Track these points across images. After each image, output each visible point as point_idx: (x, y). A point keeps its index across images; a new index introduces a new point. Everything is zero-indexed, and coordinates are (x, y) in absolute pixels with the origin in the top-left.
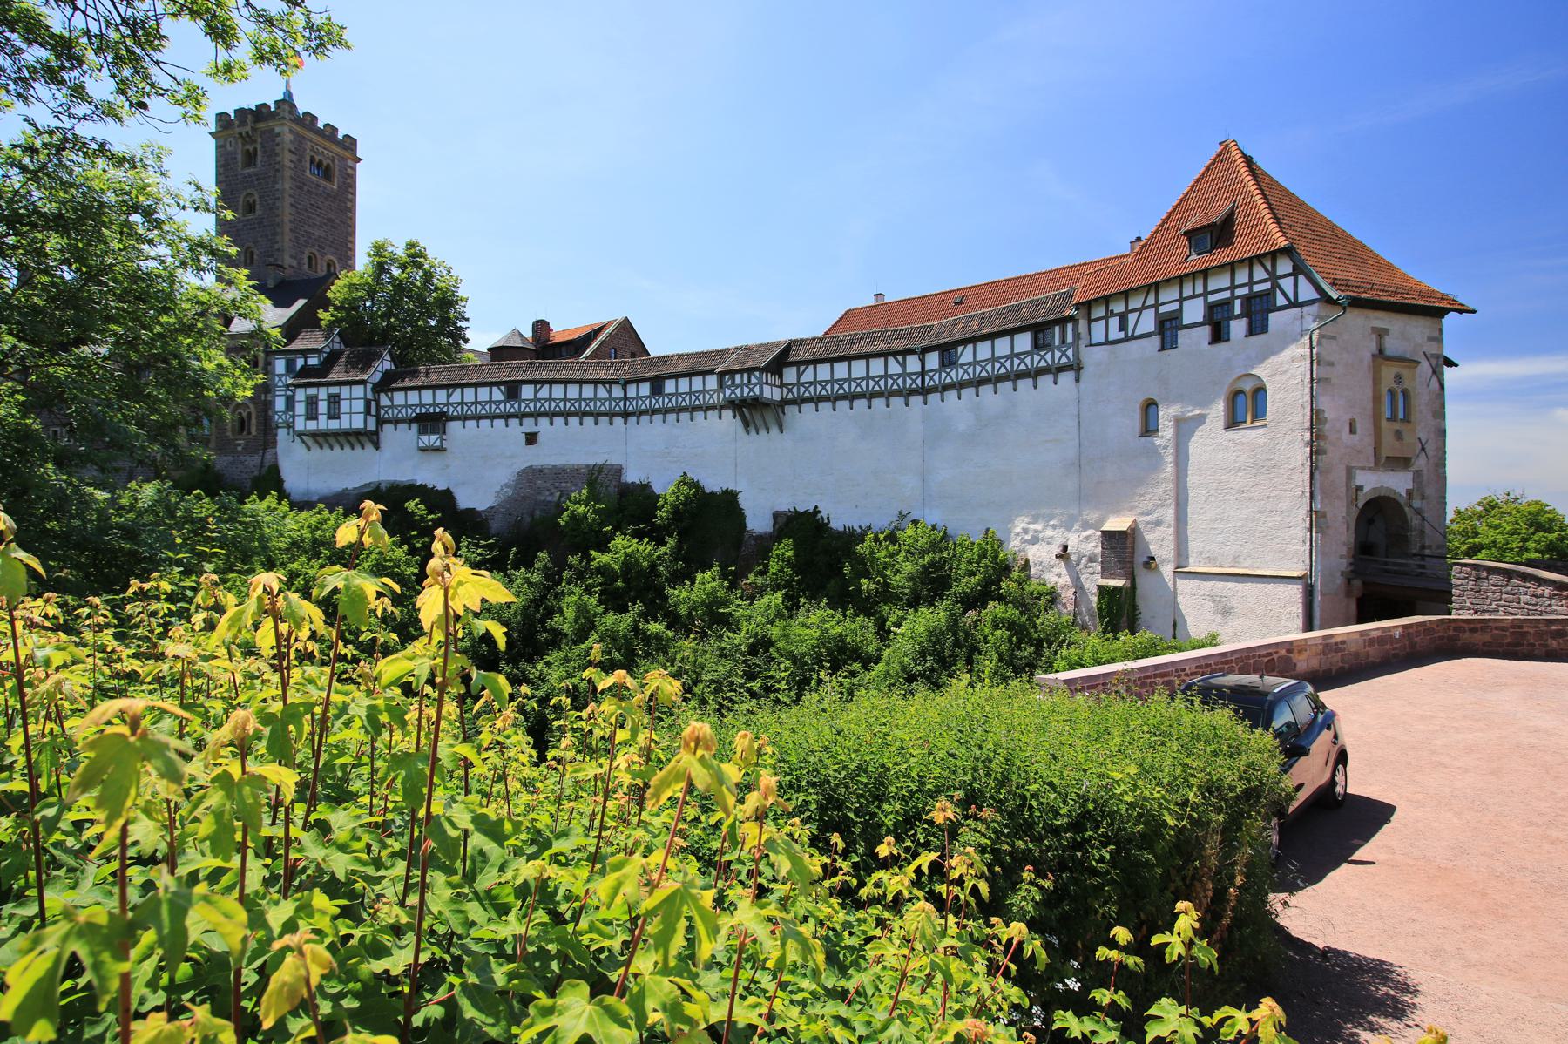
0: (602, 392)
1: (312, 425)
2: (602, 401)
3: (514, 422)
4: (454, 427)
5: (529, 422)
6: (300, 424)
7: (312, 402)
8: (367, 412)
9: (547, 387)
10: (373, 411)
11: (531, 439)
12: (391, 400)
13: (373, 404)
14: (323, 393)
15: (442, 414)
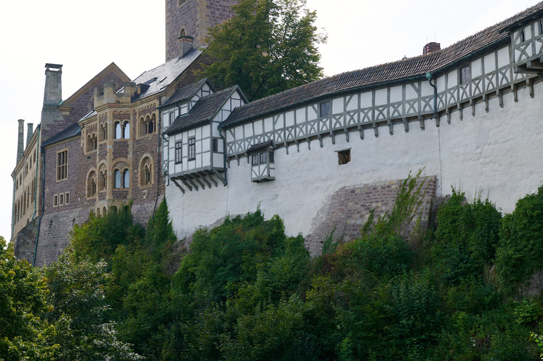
0: (410, 92)
1: (178, 169)
2: (411, 103)
3: (327, 140)
4: (280, 153)
5: (341, 138)
6: (171, 172)
7: (178, 147)
8: (214, 148)
9: (355, 97)
10: (220, 148)
11: (344, 156)
12: (234, 135)
13: (220, 142)
14: (184, 137)
15: (271, 143)
